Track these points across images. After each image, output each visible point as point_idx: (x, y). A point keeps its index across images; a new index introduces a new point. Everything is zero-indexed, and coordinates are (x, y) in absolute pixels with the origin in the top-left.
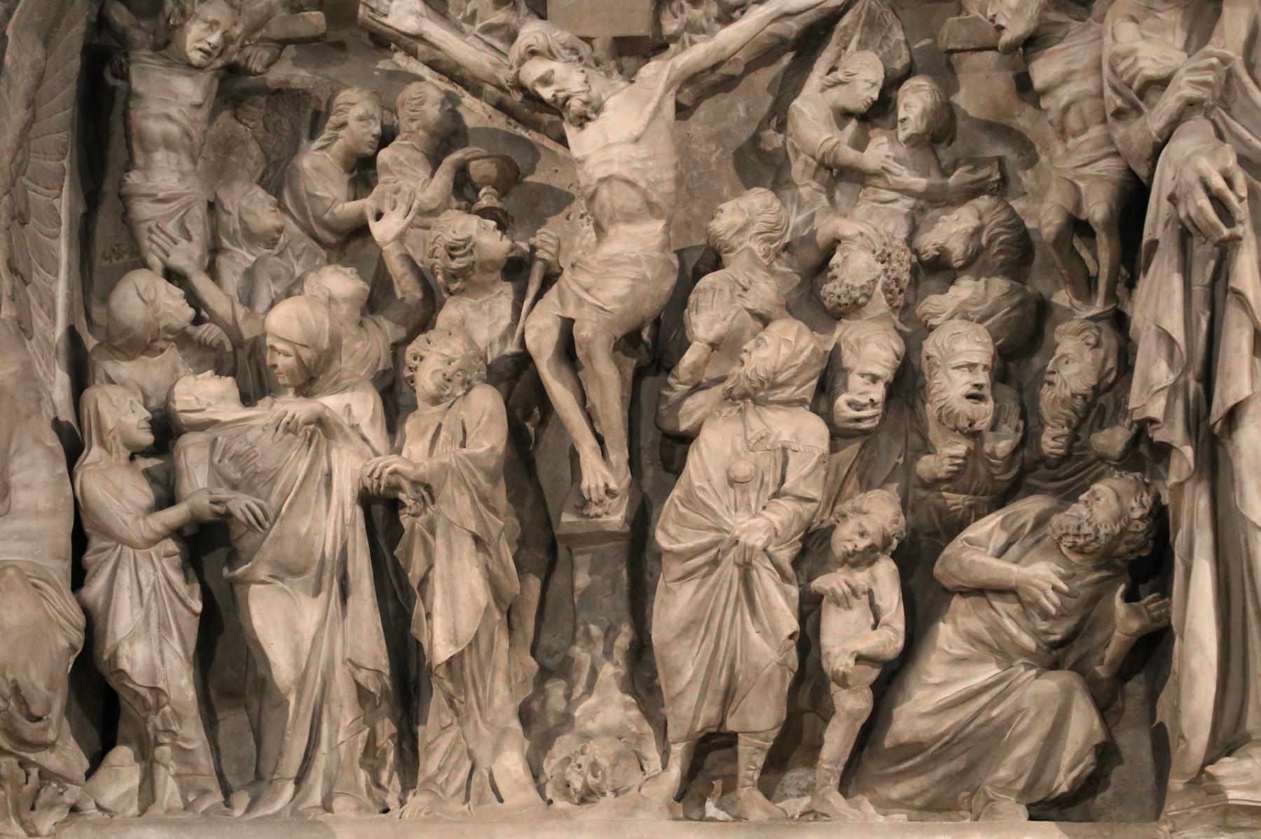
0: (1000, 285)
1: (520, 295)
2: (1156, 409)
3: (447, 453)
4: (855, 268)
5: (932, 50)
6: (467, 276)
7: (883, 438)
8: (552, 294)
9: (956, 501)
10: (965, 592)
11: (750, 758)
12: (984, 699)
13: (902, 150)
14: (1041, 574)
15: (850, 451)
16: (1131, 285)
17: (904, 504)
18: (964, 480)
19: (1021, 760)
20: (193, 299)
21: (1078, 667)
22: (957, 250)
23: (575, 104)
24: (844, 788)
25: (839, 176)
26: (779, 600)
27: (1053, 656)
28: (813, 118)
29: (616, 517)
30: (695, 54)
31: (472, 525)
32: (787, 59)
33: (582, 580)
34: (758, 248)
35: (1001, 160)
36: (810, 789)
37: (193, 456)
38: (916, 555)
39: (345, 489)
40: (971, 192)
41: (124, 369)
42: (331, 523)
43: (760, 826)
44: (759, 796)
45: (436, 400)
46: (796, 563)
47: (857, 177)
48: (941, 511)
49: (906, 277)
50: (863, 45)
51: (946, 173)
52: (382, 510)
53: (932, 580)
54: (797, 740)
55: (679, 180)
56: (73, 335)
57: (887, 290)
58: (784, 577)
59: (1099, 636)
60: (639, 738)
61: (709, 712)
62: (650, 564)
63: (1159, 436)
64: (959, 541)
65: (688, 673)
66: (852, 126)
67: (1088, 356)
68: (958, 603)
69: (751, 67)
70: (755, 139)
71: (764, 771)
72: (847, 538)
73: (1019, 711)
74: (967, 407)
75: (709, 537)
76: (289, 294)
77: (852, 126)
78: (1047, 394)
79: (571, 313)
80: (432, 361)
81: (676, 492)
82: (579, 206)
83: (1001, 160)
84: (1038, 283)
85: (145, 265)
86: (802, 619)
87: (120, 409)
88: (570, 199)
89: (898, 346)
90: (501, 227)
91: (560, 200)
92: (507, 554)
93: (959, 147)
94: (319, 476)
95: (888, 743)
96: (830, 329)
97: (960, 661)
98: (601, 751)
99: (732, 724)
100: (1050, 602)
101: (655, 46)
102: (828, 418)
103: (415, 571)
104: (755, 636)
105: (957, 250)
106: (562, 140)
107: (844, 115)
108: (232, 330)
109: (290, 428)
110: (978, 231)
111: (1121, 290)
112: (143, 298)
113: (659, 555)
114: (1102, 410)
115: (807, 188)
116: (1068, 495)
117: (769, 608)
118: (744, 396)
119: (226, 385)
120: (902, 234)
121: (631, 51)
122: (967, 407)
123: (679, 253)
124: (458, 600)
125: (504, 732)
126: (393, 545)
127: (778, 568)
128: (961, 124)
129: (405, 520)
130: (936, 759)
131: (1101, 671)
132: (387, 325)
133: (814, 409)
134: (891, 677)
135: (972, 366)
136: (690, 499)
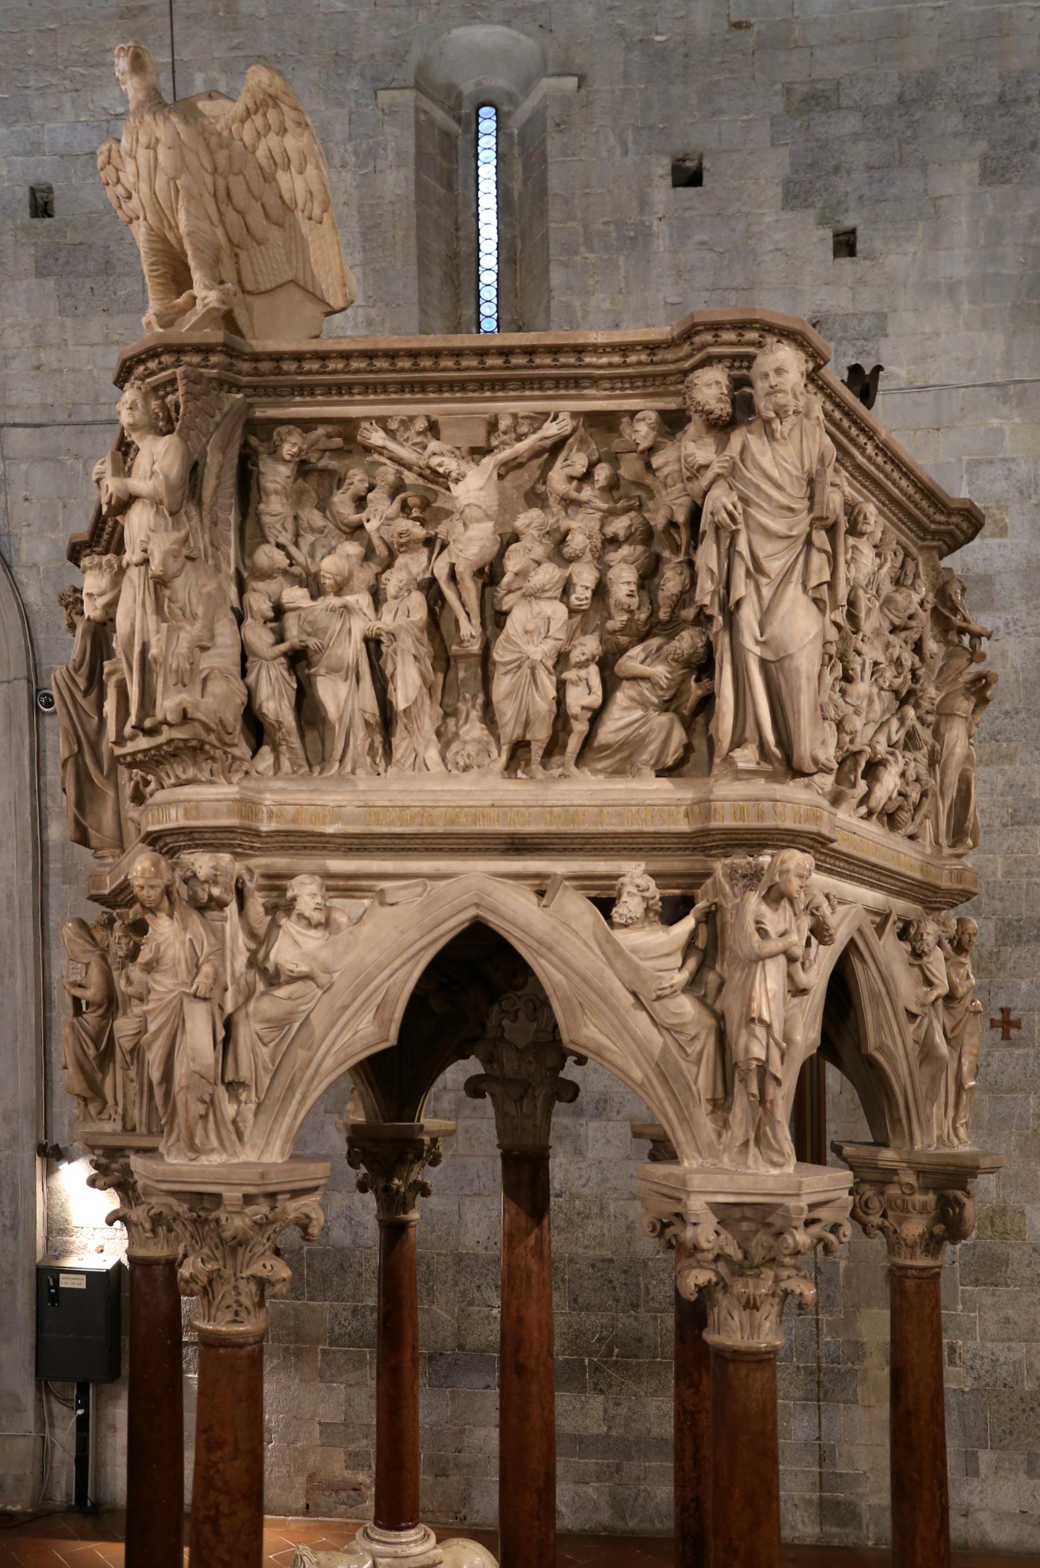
0: (640, 548)
1: (431, 553)
2: (707, 601)
3: (401, 620)
4: (577, 541)
5: (608, 453)
6: (408, 545)
7: (592, 613)
8: (445, 553)
9: (623, 640)
10: (628, 679)
11: (537, 752)
12: (637, 725)
13: (597, 493)
14: (660, 671)
15: (577, 618)
16: (696, 548)
17: (601, 641)
18: (627, 631)
19: (652, 752)
20: (289, 556)
21: (676, 711)
22: (622, 534)
23: (454, 475)
24: (577, 764)
25: (569, 503)
26: (547, 682)
27: (666, 706)
28: (558, 479)
29: (475, 647)
30: (506, 453)
31: (413, 651)
32: (546, 456)
33: (461, 674)
34: (535, 533)
35: (639, 497)
36: (562, 765)
37: (291, 622)
38: (607, 663)
39: (357, 635)
40: (627, 510)
41: (260, 585)
42: (351, 650)
43: (541, 781)
44: (541, 768)
45: (396, 598)
46: (555, 666)
47: (579, 504)
48: (617, 644)
49: (599, 545)
50: (579, 450)
51: (616, 502)
52: (373, 645)
53: (613, 674)
54: (557, 743)
55: (500, 505)
56: (238, 571)
57: (591, 551)
58: (550, 673)
59: (685, 697)
60: (488, 743)
61: (518, 732)
62: (491, 667)
63: (708, 612)
64: (625, 657)
65: (509, 715)
66: (575, 483)
67: (678, 578)
68: (625, 684)
69: (530, 459)
70: (533, 488)
71: (543, 757)
72: (576, 656)
73: (651, 730)
74: (627, 600)
75: (517, 655)
76: (330, 553)
77: (575, 483)
78: (661, 595)
79: (454, 561)
80: (393, 581)
81: (502, 637)
82: (456, 516)
83: (639, 497)
84: (656, 548)
85: (267, 542)
86: (558, 690)
87: (259, 602)
88: (452, 513)
89: (596, 574)
90: (422, 525)
91: (448, 513)
92: (429, 663)
93: (621, 492)
94: (346, 630)
95: (596, 744)
96: (567, 567)
97: (626, 708)
98: (472, 749)
99: (528, 737)
100: (664, 683)
101: (488, 451)
102: (568, 606)
103: (388, 672)
104: (537, 698)
105: (622, 534)
106: (448, 489)
107: (571, 478)
108: (306, 569)
109: (333, 610)
110: (630, 526)
111: (691, 551)
112: (267, 556)
113: (495, 663)
114: (684, 601)
115: (556, 508)
116: (671, 637)
117: (544, 686)
118: (531, 595)
119: (304, 592)
120: (598, 527)
121: (477, 453)
122: (627, 600)
123: (501, 535)
124: (407, 684)
125: (429, 741)
126: (378, 660)
127: (547, 668)
128: (622, 482)
129: (384, 648)
130: (618, 750)
131: (686, 712)
132: (373, 566)
133: (561, 601)
134: (597, 716)
135: (629, 583)
136: (508, 639)
